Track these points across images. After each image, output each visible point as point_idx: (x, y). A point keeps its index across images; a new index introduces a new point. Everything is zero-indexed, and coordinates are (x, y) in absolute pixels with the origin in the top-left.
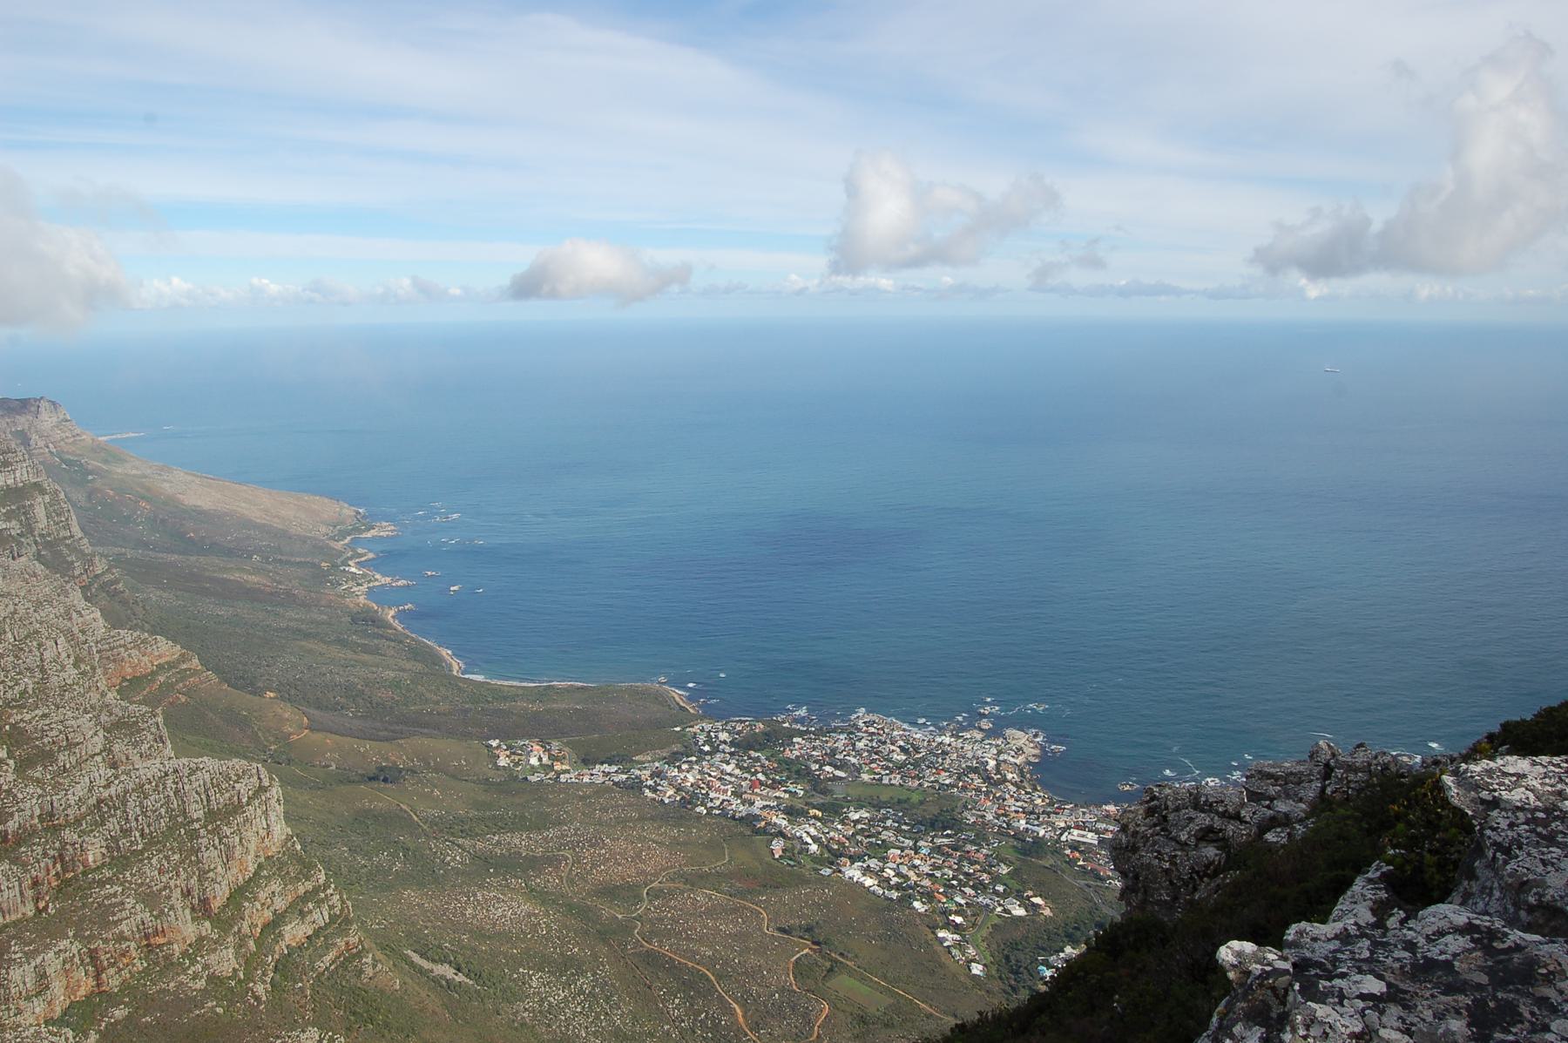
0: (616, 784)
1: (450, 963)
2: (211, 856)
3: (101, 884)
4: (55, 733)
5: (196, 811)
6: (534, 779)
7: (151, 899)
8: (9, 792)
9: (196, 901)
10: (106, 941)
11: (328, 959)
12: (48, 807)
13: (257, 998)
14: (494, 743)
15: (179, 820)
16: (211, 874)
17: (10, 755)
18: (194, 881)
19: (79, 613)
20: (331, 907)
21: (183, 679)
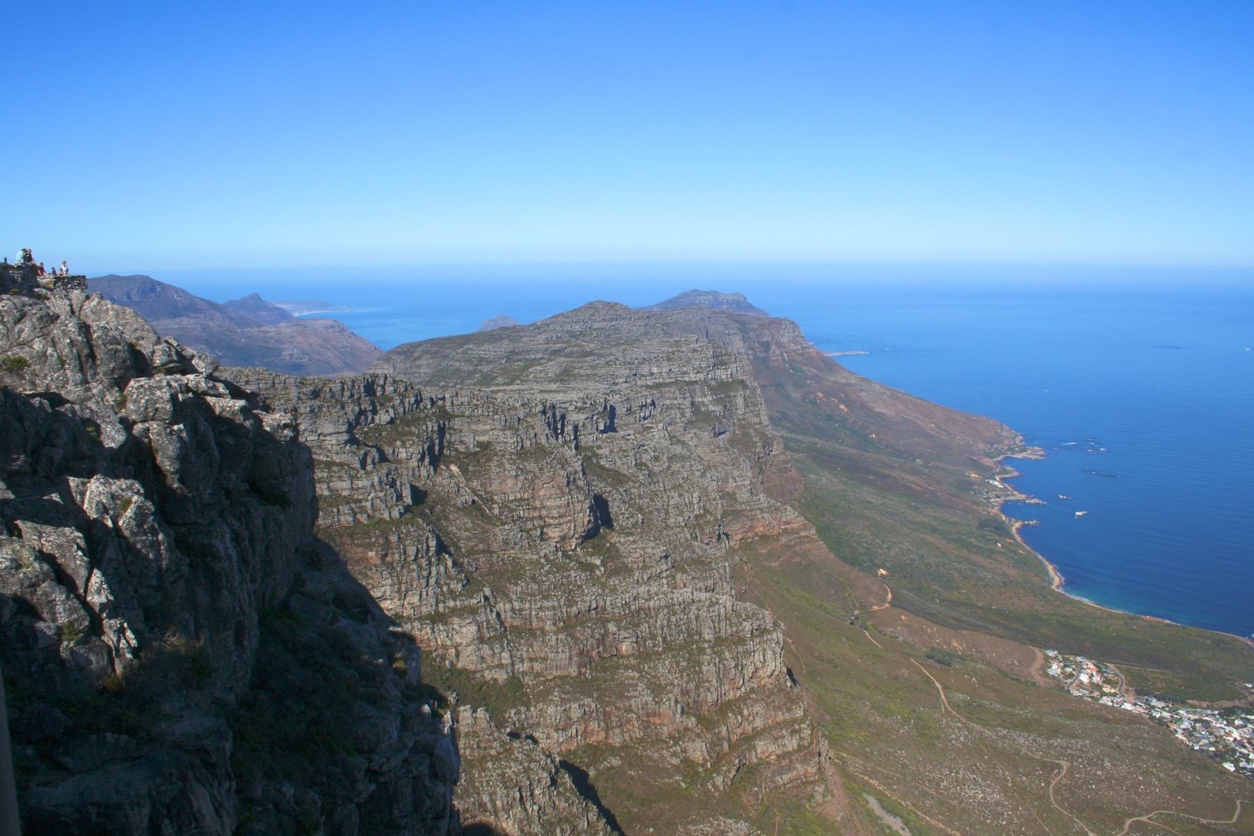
0: (1152, 718)
1: (902, 817)
2: (708, 669)
3: (627, 668)
4: (637, 555)
5: (708, 635)
6: (1075, 693)
7: (657, 689)
8: (580, 587)
9: (691, 701)
10: (618, 708)
11: (786, 778)
12: (601, 604)
13: (716, 788)
14: (1051, 653)
15: (693, 635)
16: (707, 684)
17: (604, 563)
18: (692, 686)
19: (734, 479)
20: (801, 739)
21: (801, 543)
